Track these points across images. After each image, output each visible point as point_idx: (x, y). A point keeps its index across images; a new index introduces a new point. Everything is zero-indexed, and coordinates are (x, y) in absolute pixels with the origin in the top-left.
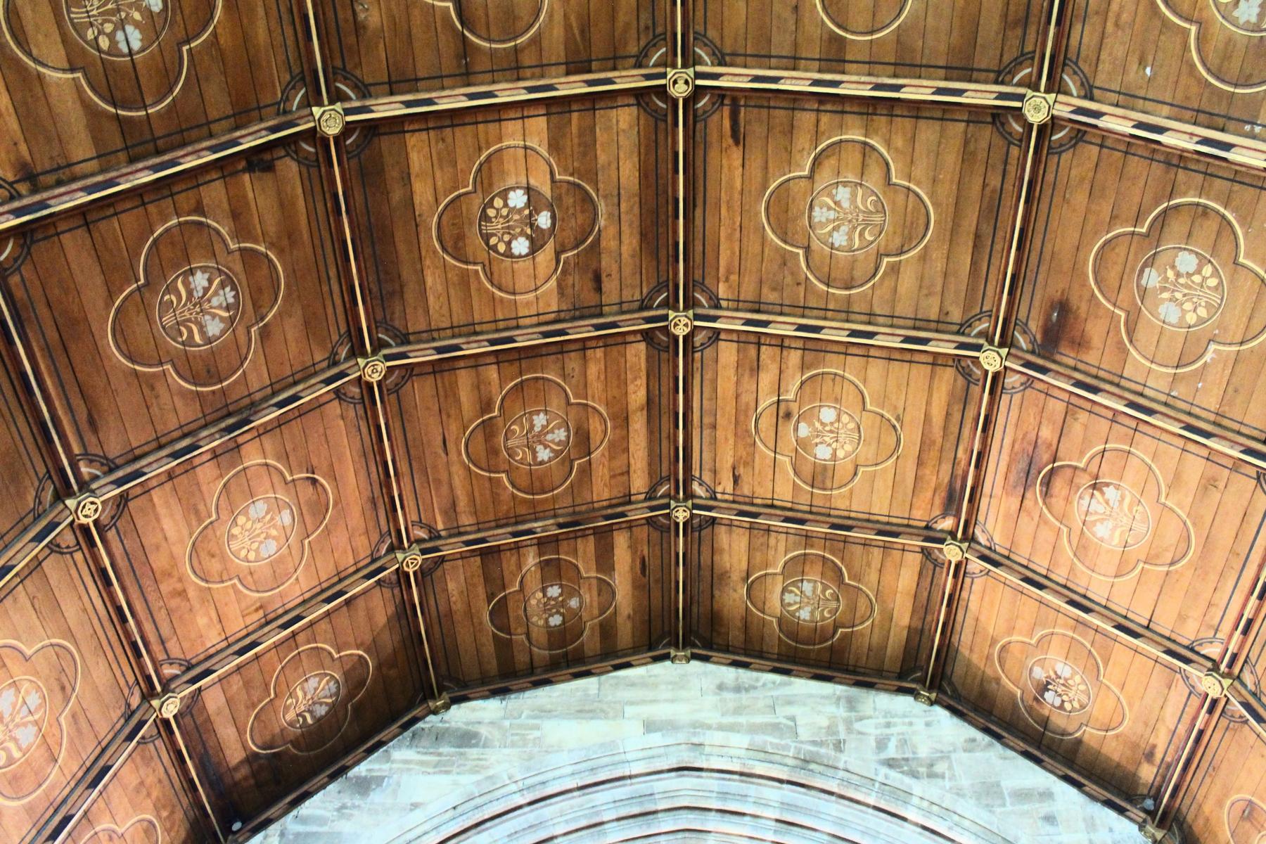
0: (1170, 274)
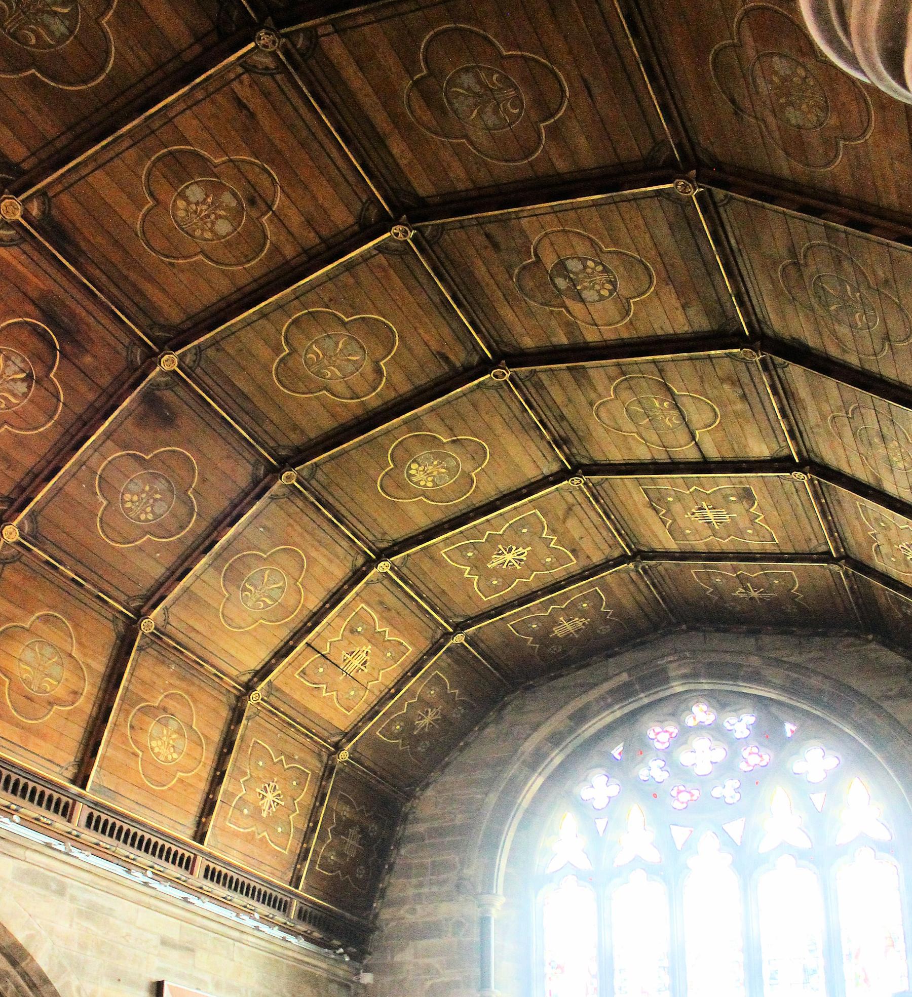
0: (158, 496)
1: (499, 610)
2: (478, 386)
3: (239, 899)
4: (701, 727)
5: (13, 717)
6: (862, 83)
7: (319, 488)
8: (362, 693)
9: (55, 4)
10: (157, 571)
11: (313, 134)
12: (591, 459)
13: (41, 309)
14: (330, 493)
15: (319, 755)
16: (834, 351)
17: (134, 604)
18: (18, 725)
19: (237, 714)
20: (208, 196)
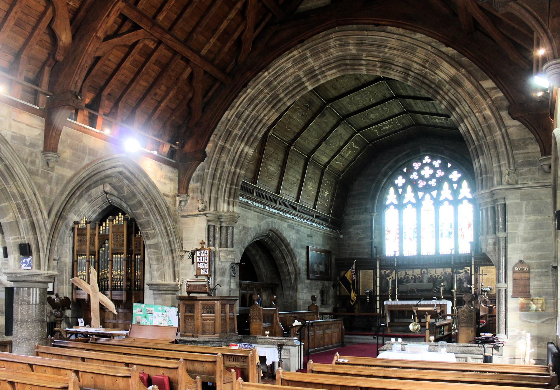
4: (427, 164)
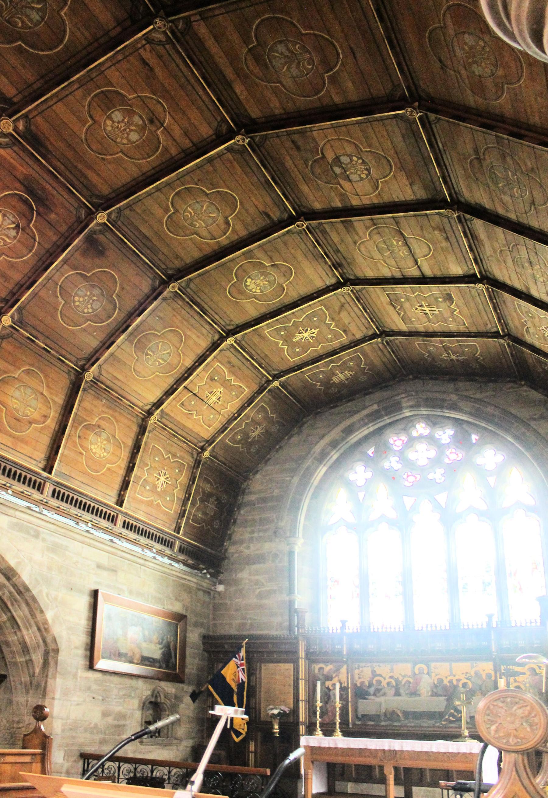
0: (95, 298)
1: (300, 367)
2: (288, 232)
3: (143, 540)
4: (421, 437)
5: (8, 431)
6: (518, 50)
7: (192, 293)
8: (217, 416)
9: (33, 2)
10: (94, 343)
11: (188, 81)
12: (355, 276)
13: (25, 186)
14: (198, 296)
15: (192, 454)
16: (501, 211)
17: (81, 363)
18: (11, 435)
19: (142, 429)
20: (125, 118)
